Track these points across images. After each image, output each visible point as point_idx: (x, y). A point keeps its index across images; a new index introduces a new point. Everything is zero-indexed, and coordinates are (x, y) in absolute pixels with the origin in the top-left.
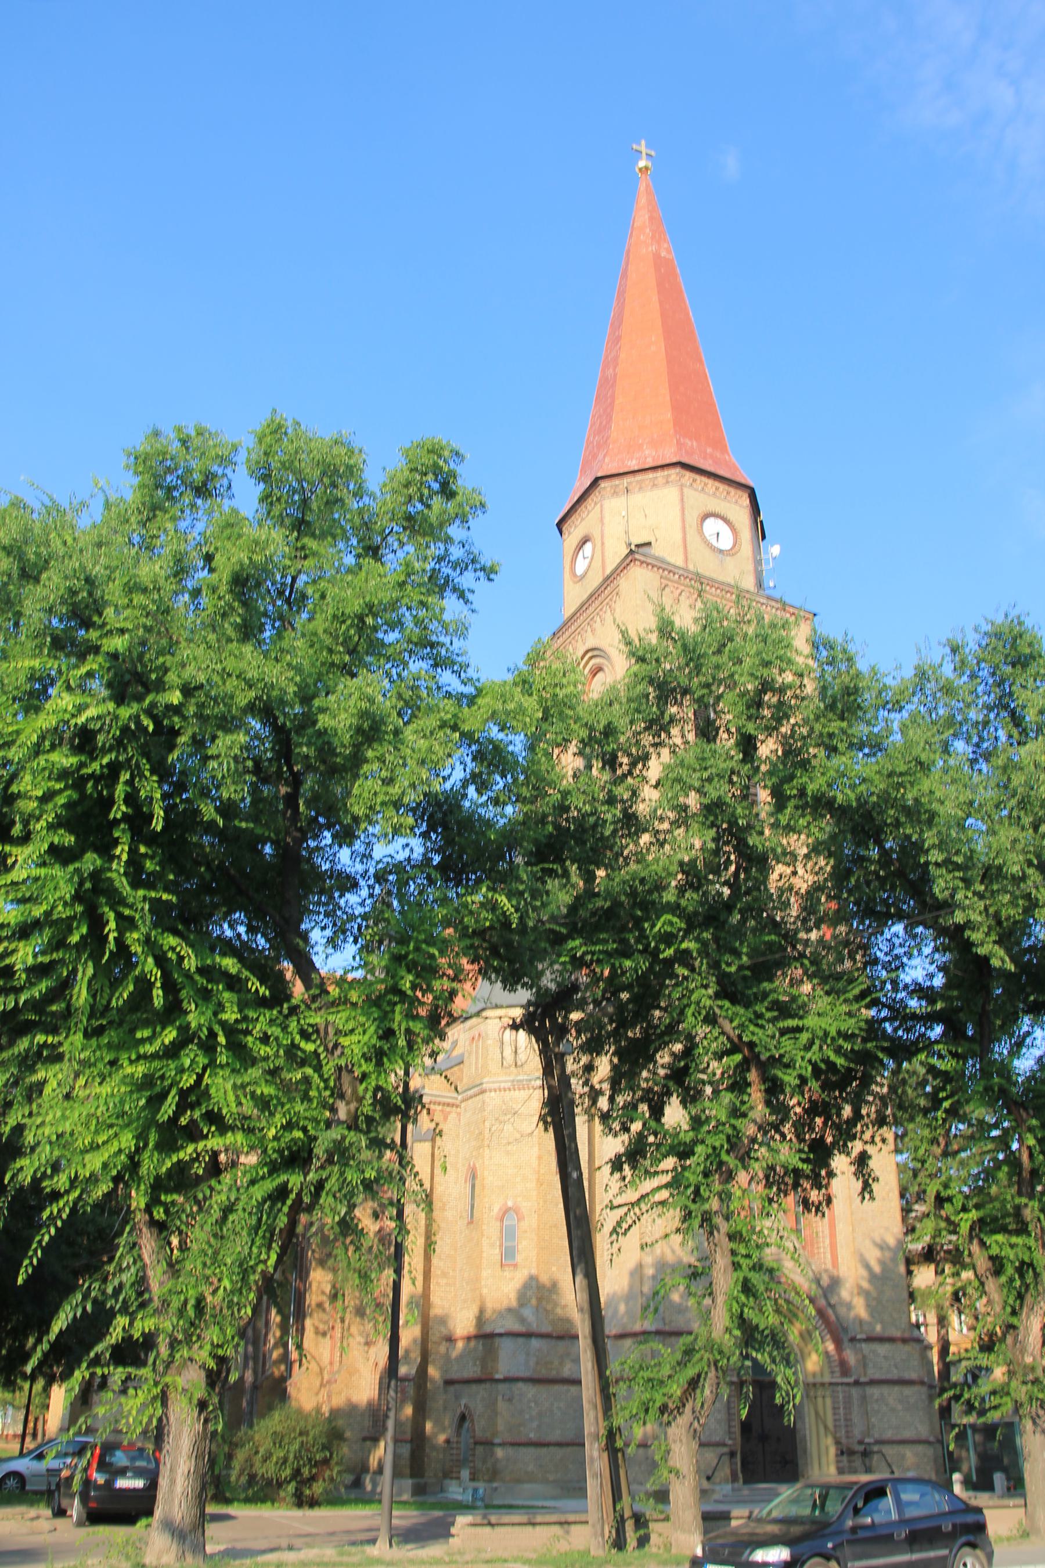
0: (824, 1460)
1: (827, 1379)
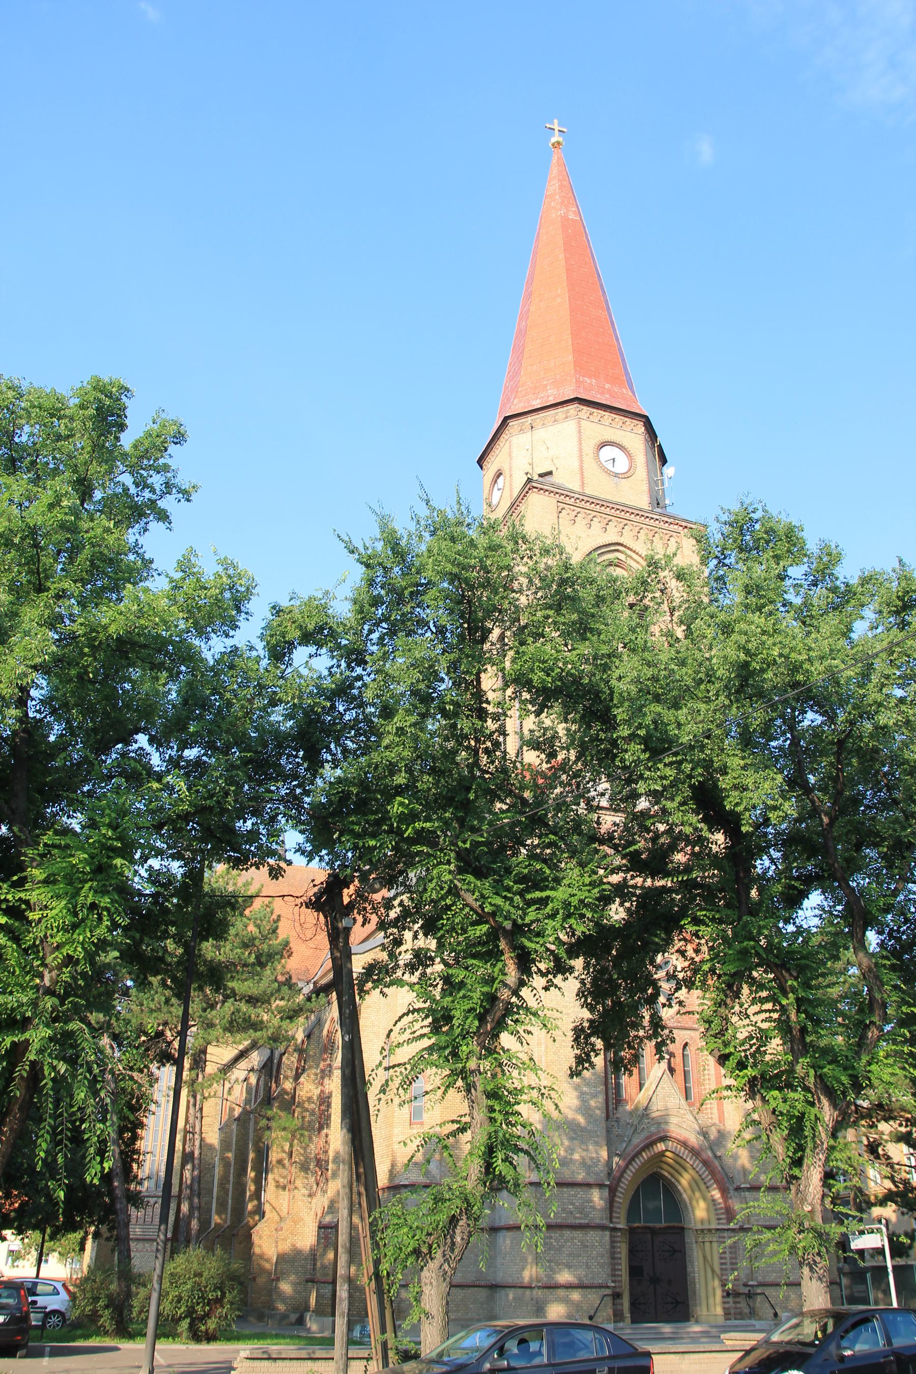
0: (711, 1301)
1: (714, 1226)
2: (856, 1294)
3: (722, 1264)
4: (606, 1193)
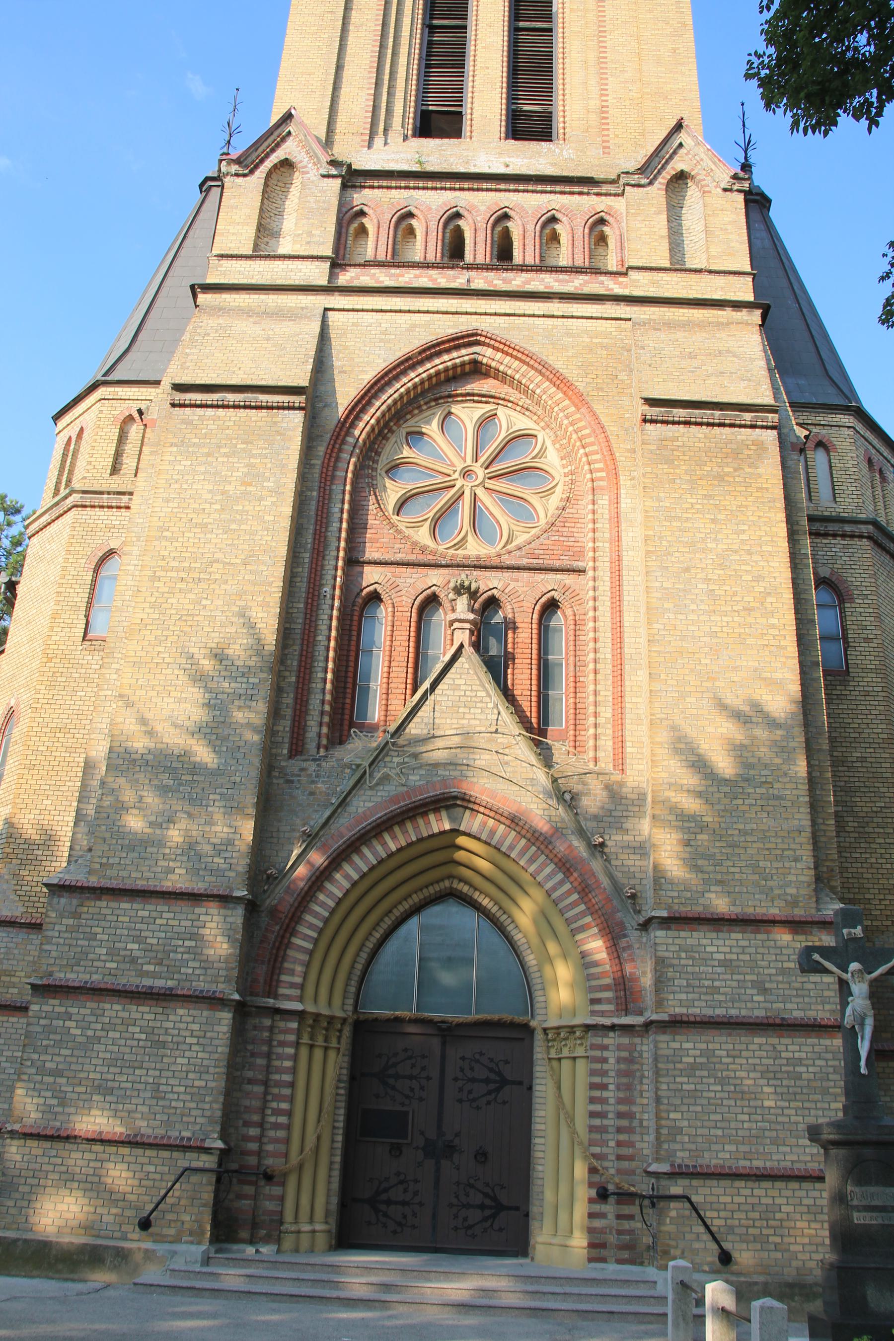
0: (563, 1216)
1: (581, 1019)
2: (859, 1218)
3: (593, 1115)
4: (237, 916)
